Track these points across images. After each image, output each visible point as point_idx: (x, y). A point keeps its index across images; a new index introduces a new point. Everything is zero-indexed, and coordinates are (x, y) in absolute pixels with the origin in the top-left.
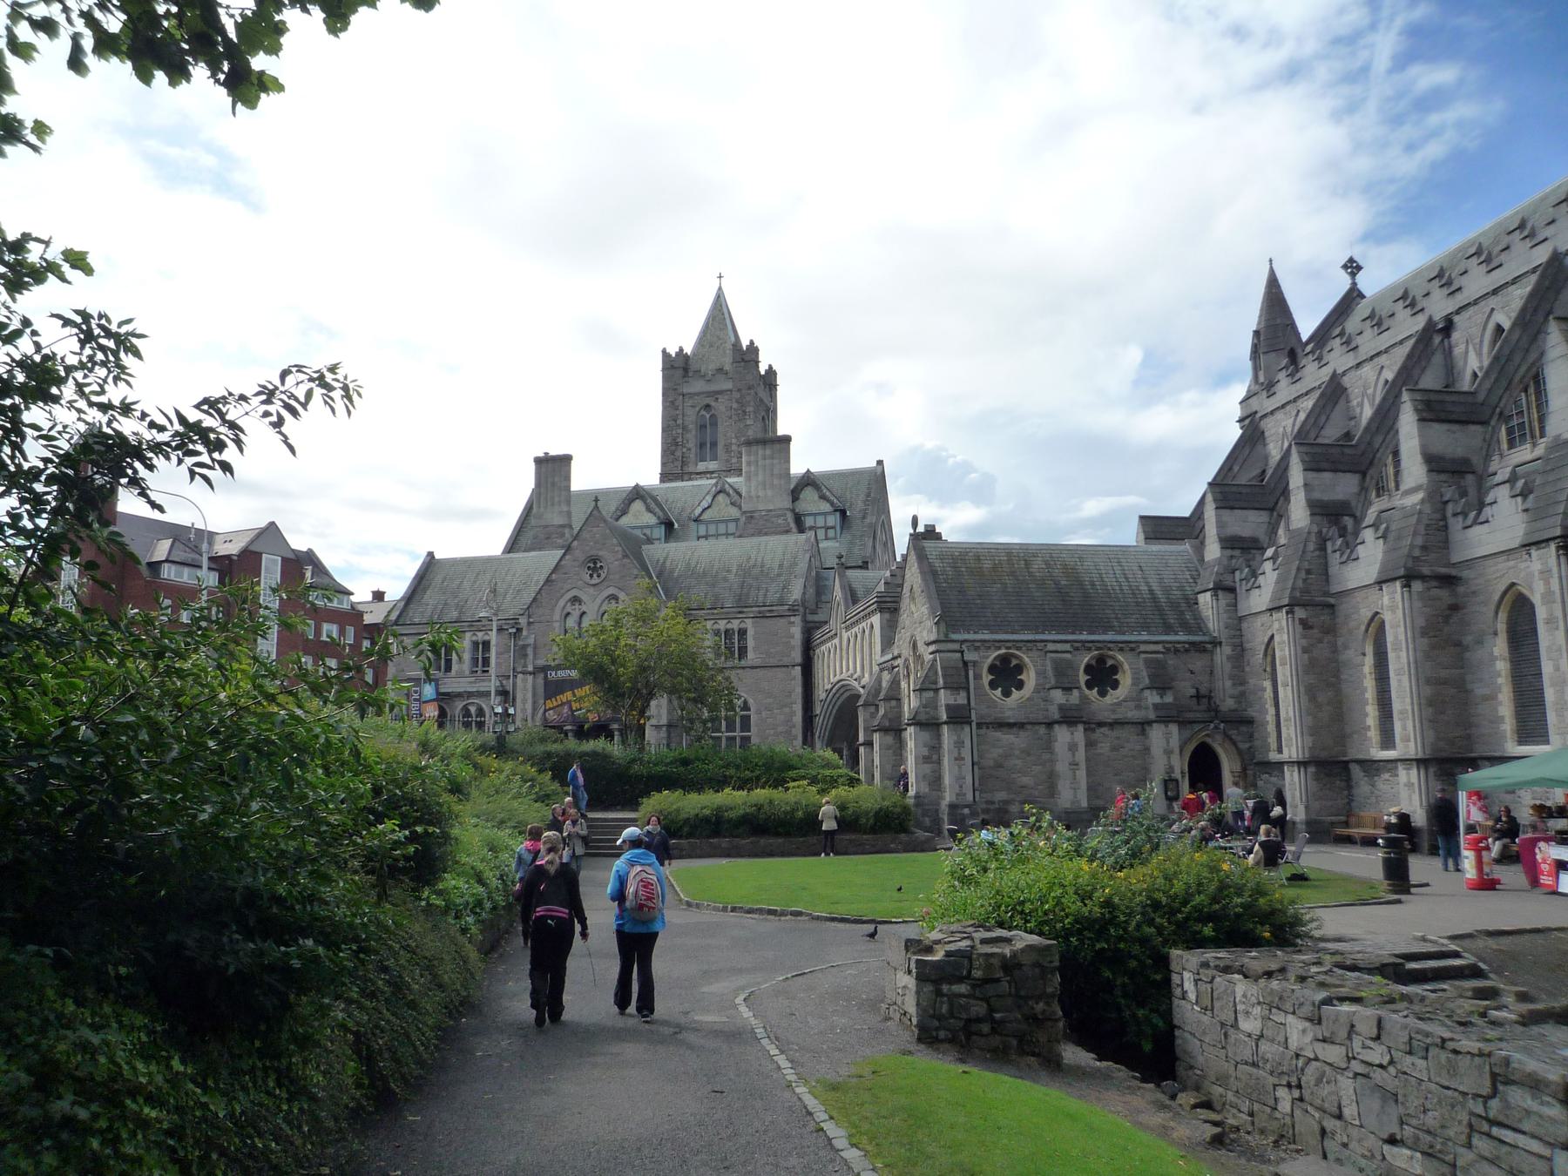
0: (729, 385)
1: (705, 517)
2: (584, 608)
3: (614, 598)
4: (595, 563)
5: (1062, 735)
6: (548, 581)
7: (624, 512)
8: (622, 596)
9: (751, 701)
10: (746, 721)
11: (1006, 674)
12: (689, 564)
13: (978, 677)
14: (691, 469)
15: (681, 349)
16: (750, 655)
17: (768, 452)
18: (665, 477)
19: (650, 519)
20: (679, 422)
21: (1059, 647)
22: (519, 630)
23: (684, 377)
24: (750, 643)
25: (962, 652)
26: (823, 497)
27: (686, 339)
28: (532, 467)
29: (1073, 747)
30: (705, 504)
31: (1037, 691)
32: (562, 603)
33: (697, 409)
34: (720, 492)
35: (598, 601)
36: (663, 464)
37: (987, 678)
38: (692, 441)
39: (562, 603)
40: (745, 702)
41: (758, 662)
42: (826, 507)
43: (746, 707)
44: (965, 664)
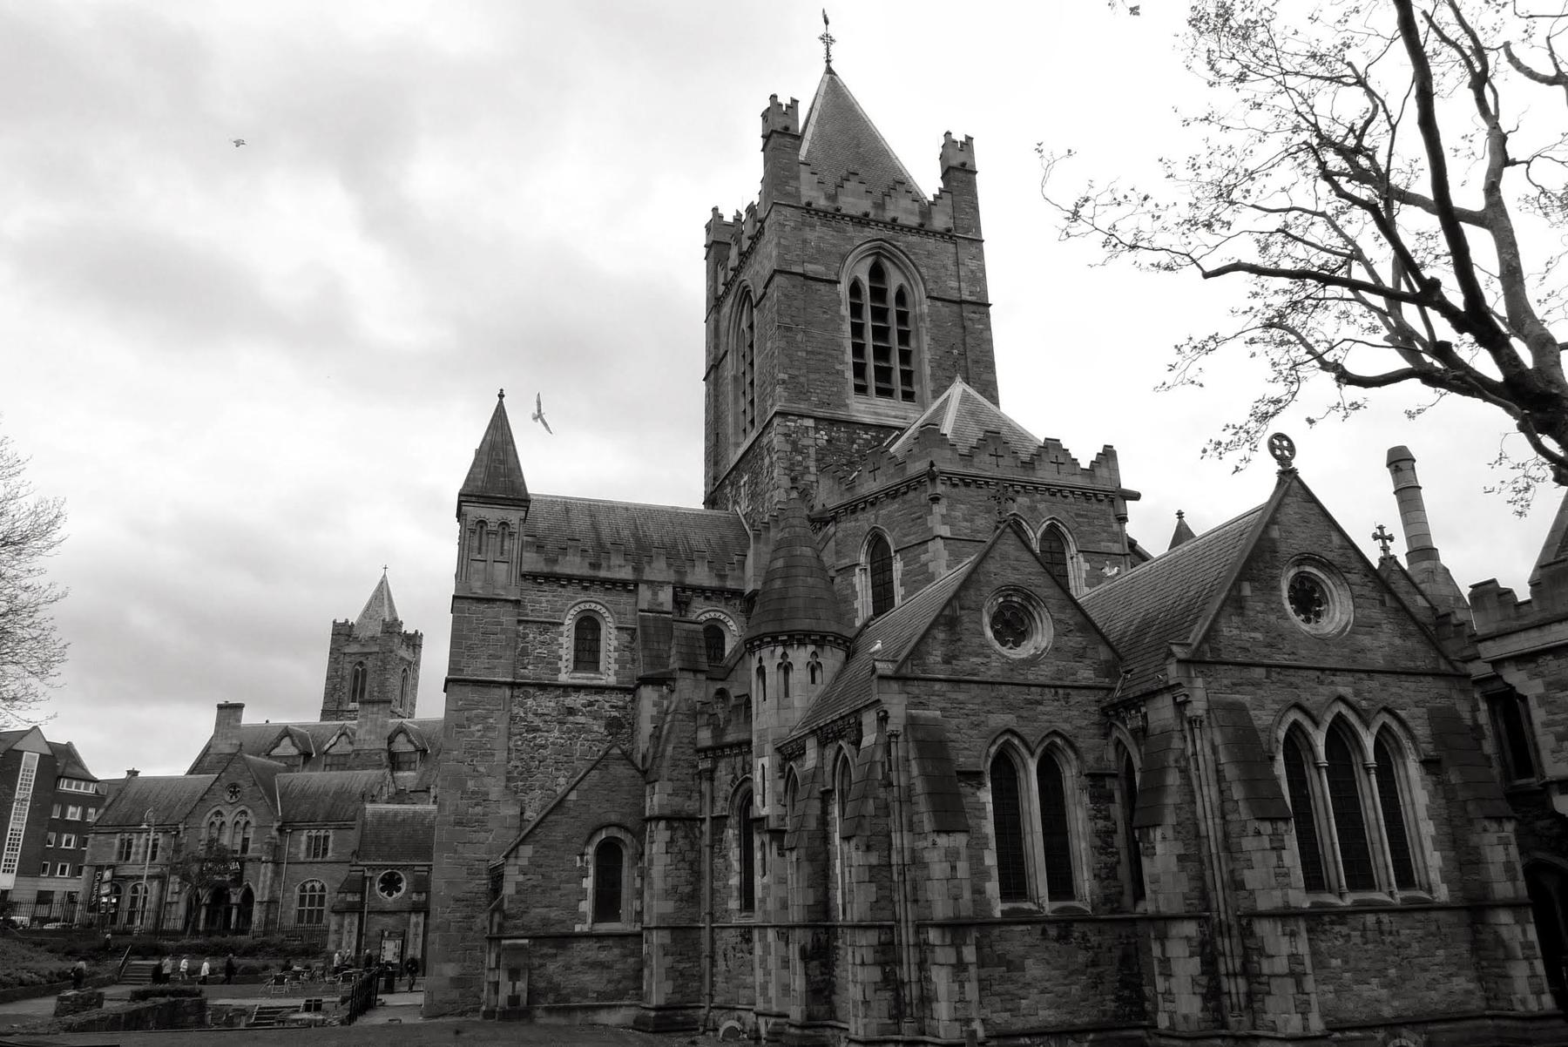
1: (331, 751)
2: (223, 819)
3: (244, 813)
5: (413, 918)
6: (202, 799)
7: (277, 745)
8: (249, 811)
9: (326, 885)
10: (322, 898)
11: (391, 884)
12: (303, 790)
13: (372, 885)
14: (345, 708)
15: (347, 621)
16: (329, 854)
17: (375, 709)
18: (325, 714)
19: (293, 751)
21: (420, 869)
22: (178, 832)
24: (331, 846)
25: (364, 871)
26: (410, 741)
27: (352, 614)
28: (215, 711)
29: (417, 925)
30: (332, 742)
31: (405, 893)
32: (209, 815)
34: (342, 734)
35: (234, 814)
36: (325, 703)
37: (377, 887)
38: (347, 686)
39: (209, 815)
40: (323, 886)
41: (333, 859)
42: (411, 748)
43: (323, 887)
44: (365, 878)
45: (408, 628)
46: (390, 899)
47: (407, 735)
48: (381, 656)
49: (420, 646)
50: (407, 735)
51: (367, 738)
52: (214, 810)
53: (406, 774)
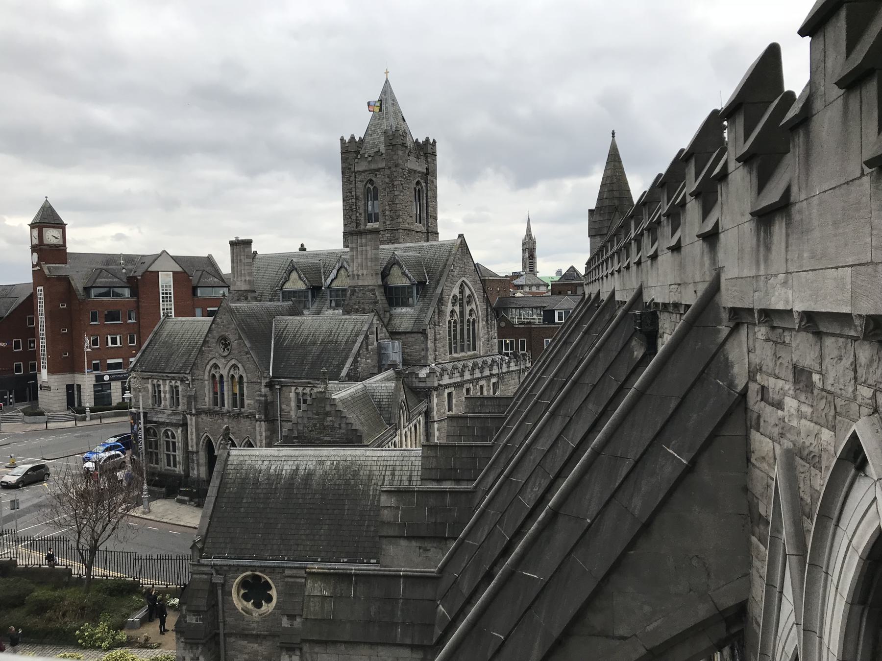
0: (382, 165)
4: (226, 341)
7: (287, 280)
8: (240, 365)
20: (353, 193)
23: (356, 158)
28: (229, 247)
30: (332, 276)
32: (208, 367)
33: (364, 183)
34: (341, 267)
35: (227, 368)
36: (345, 225)
39: (208, 367)
44: (214, 586)
45: (418, 135)
46: (256, 613)
47: (401, 267)
48: (388, 172)
49: (434, 154)
50: (401, 267)
51: (360, 273)
52: (211, 363)
53: (405, 310)
